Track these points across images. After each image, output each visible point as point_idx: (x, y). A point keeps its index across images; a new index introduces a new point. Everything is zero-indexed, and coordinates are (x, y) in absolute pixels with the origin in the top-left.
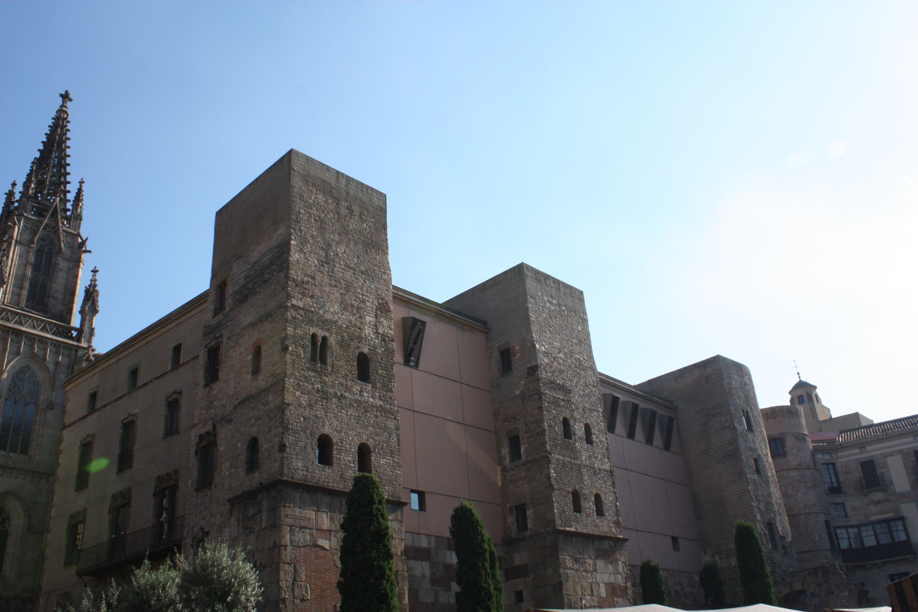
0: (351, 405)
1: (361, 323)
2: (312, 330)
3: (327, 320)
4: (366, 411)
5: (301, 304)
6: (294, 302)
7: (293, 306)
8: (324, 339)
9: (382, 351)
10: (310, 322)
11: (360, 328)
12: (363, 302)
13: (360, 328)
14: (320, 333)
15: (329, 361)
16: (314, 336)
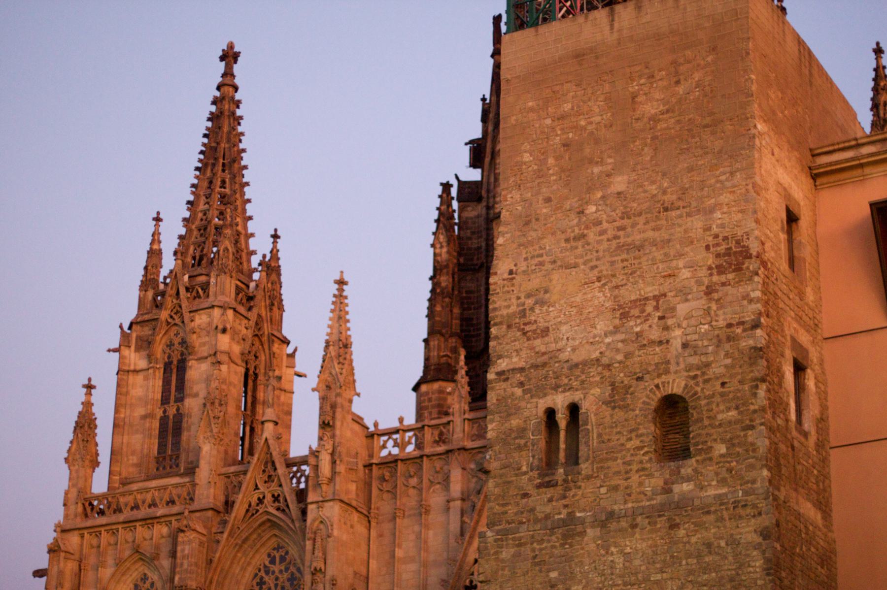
0: (634, 526)
1: (666, 328)
2: (543, 404)
3: (576, 365)
4: (674, 526)
5: (517, 361)
6: (503, 365)
7: (498, 374)
8: (574, 409)
9: (726, 366)
10: (540, 391)
11: (660, 343)
12: (670, 276)
13: (660, 343)
14: (560, 401)
15: (583, 450)
16: (551, 413)
